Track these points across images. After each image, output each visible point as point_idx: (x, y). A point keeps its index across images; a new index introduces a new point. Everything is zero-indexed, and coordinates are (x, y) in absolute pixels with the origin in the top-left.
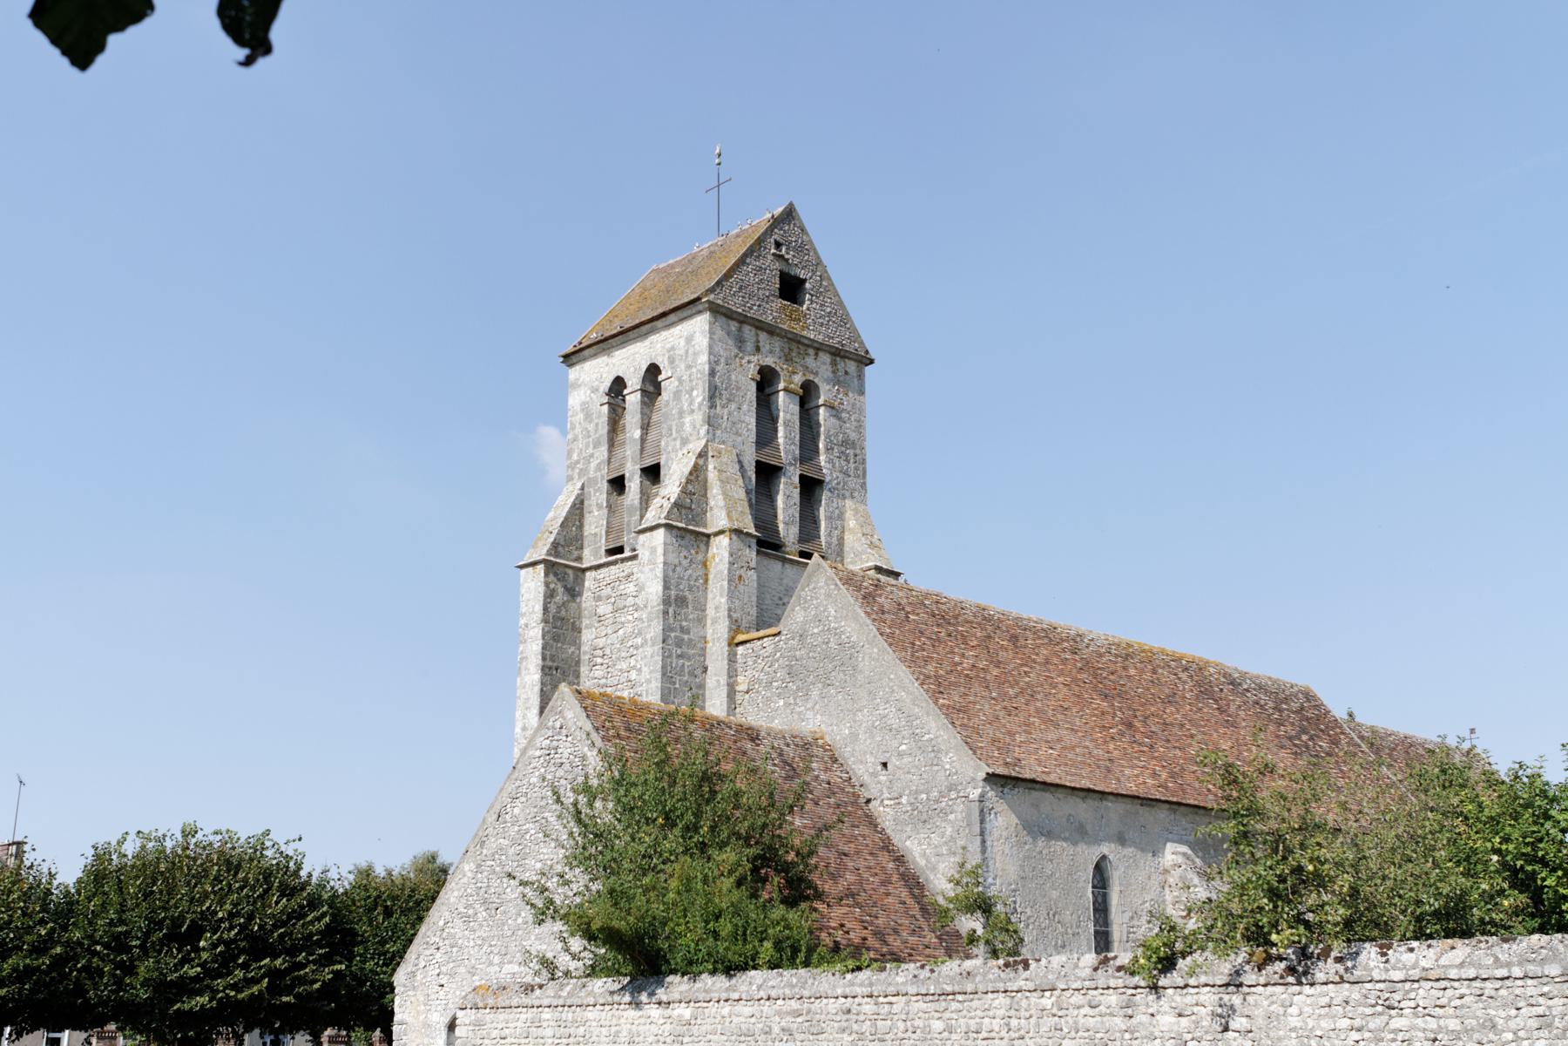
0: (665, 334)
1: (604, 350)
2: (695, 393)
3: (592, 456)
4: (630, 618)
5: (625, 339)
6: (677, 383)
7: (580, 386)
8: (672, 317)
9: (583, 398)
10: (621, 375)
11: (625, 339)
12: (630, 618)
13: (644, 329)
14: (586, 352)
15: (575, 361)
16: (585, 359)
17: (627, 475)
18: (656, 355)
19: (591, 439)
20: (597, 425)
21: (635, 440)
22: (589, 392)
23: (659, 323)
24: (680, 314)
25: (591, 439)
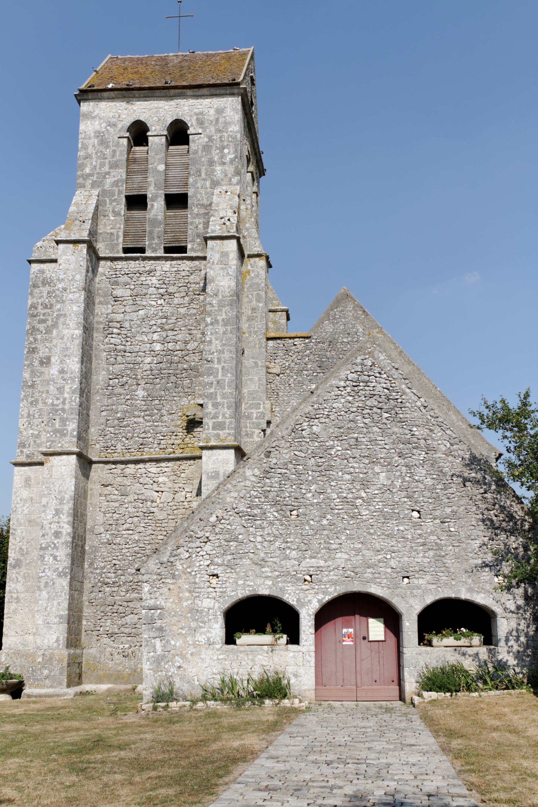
0: (191, 101)
1: (124, 97)
2: (226, 151)
3: (108, 173)
4: (154, 303)
5: (150, 94)
6: (206, 140)
7: (94, 118)
8: (205, 91)
9: (98, 128)
10: (142, 119)
11: (150, 94)
12: (154, 303)
13: (172, 92)
14: (106, 94)
15: (90, 97)
16: (101, 99)
17: (149, 196)
18: (182, 115)
19: (107, 161)
20: (114, 151)
21: (158, 171)
22: (104, 125)
23: (189, 92)
24: (213, 90)
25: (107, 161)
